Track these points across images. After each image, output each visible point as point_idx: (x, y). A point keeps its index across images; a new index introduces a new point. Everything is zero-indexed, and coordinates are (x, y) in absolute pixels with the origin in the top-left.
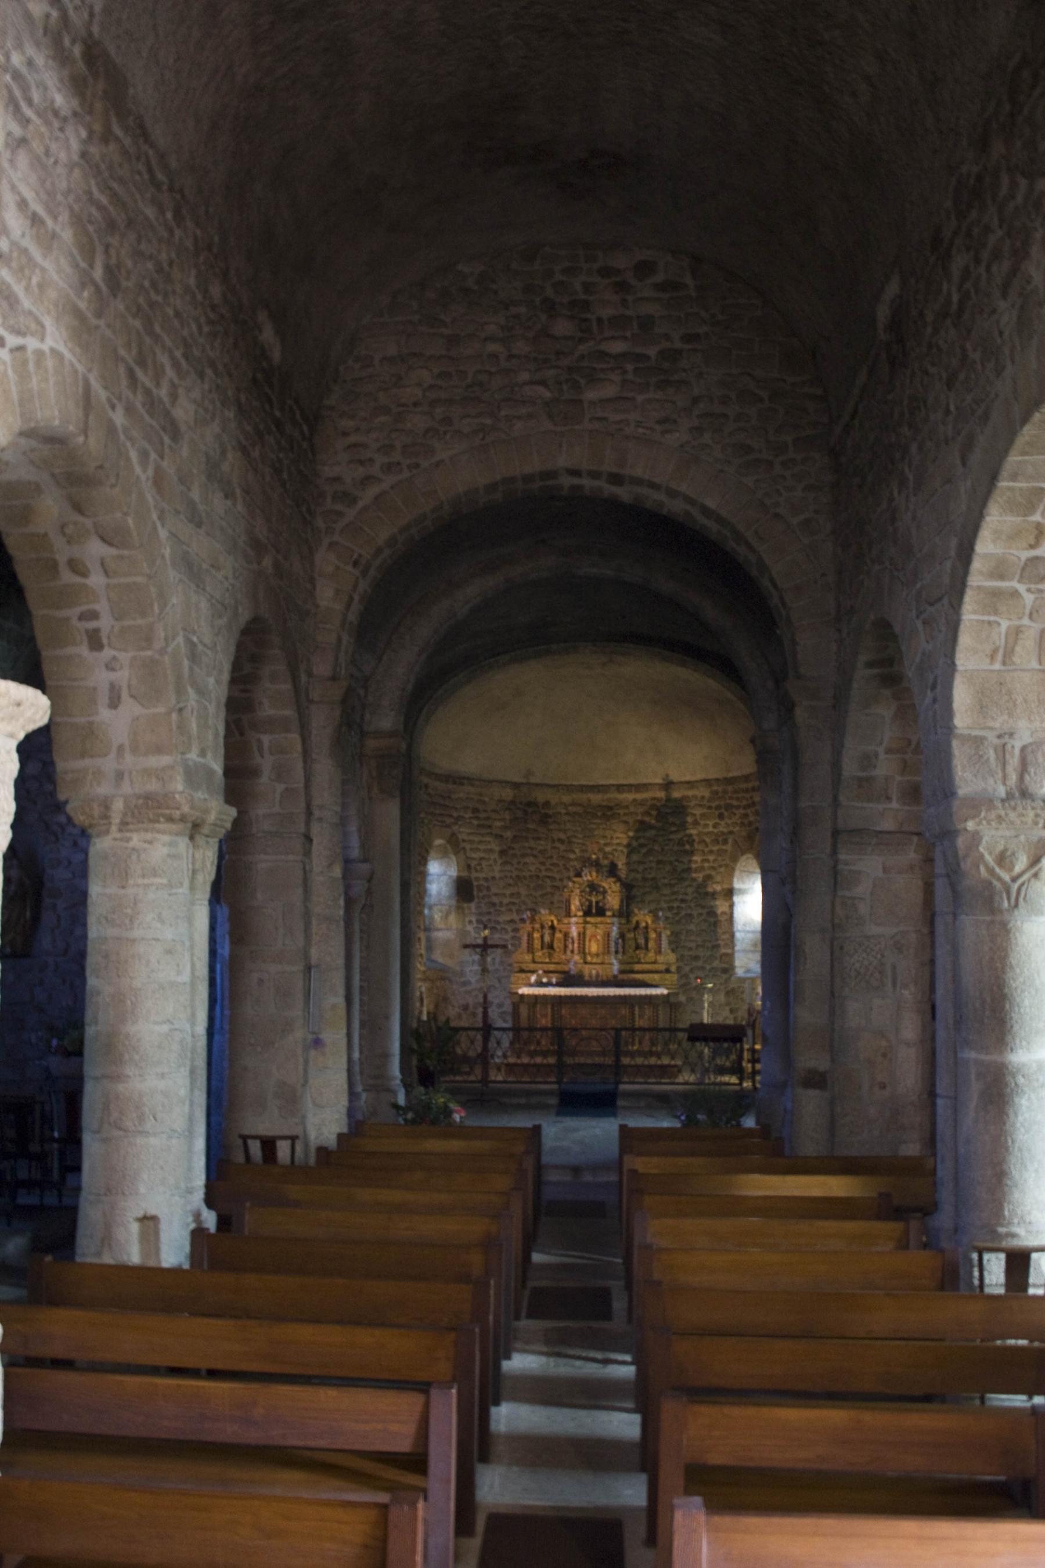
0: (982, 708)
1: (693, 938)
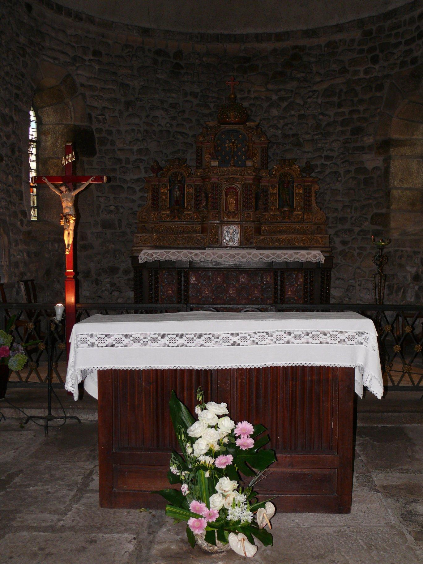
1: (339, 198)
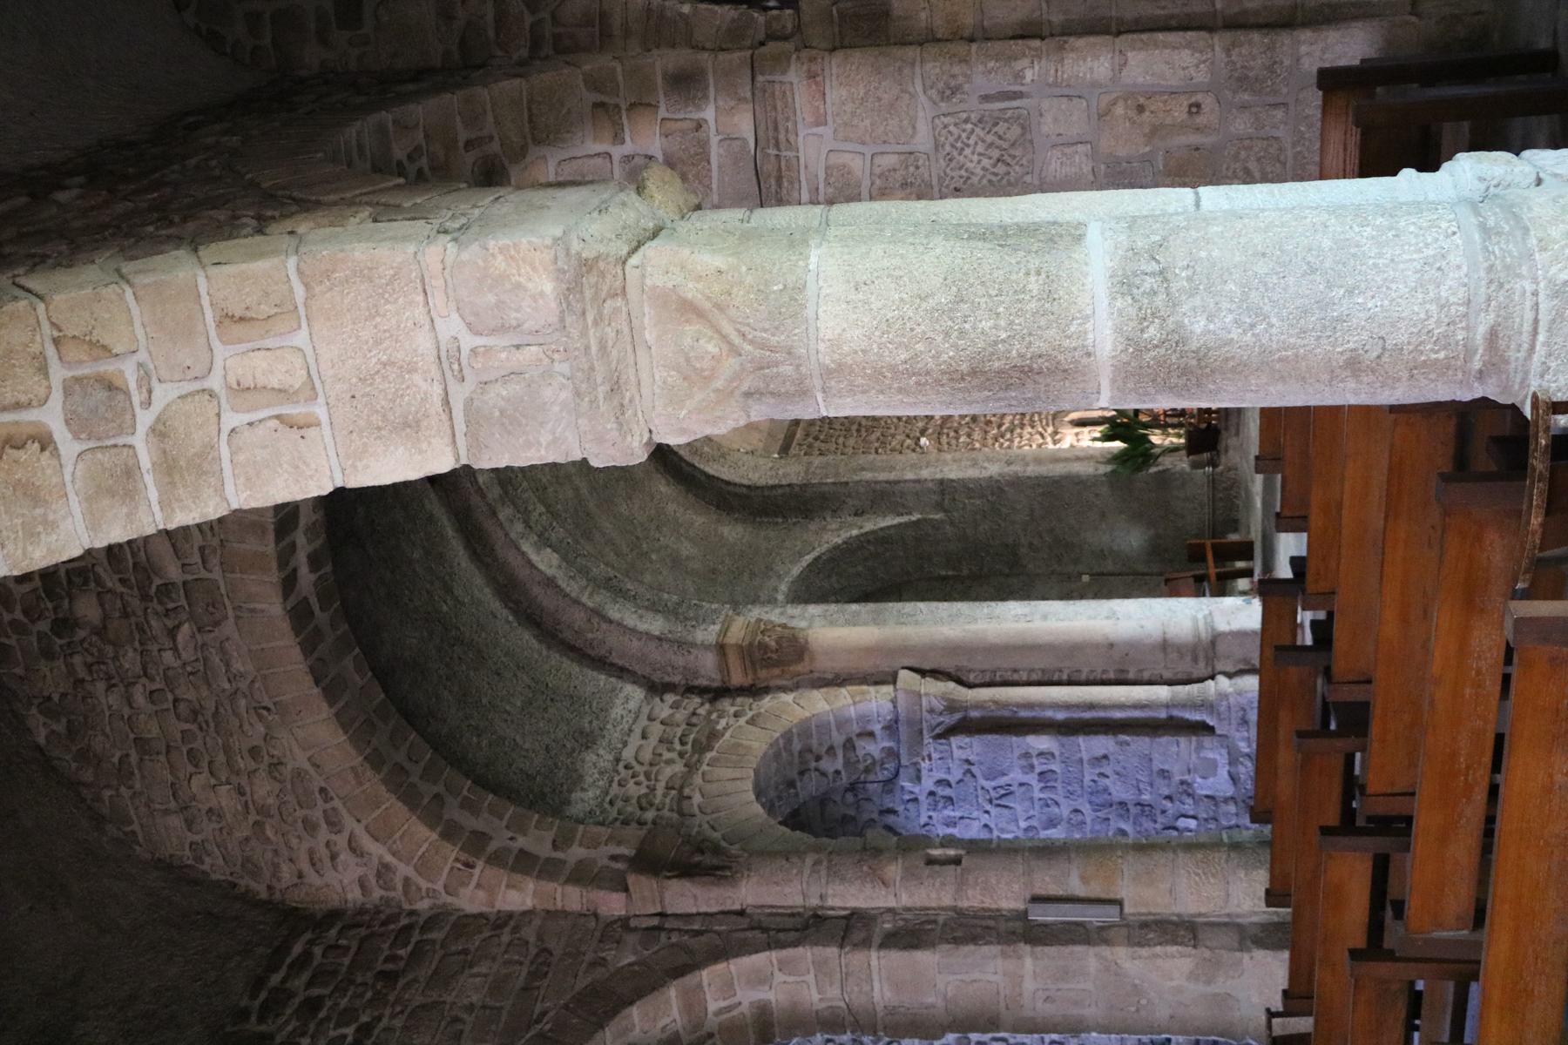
0: (410, 426)
